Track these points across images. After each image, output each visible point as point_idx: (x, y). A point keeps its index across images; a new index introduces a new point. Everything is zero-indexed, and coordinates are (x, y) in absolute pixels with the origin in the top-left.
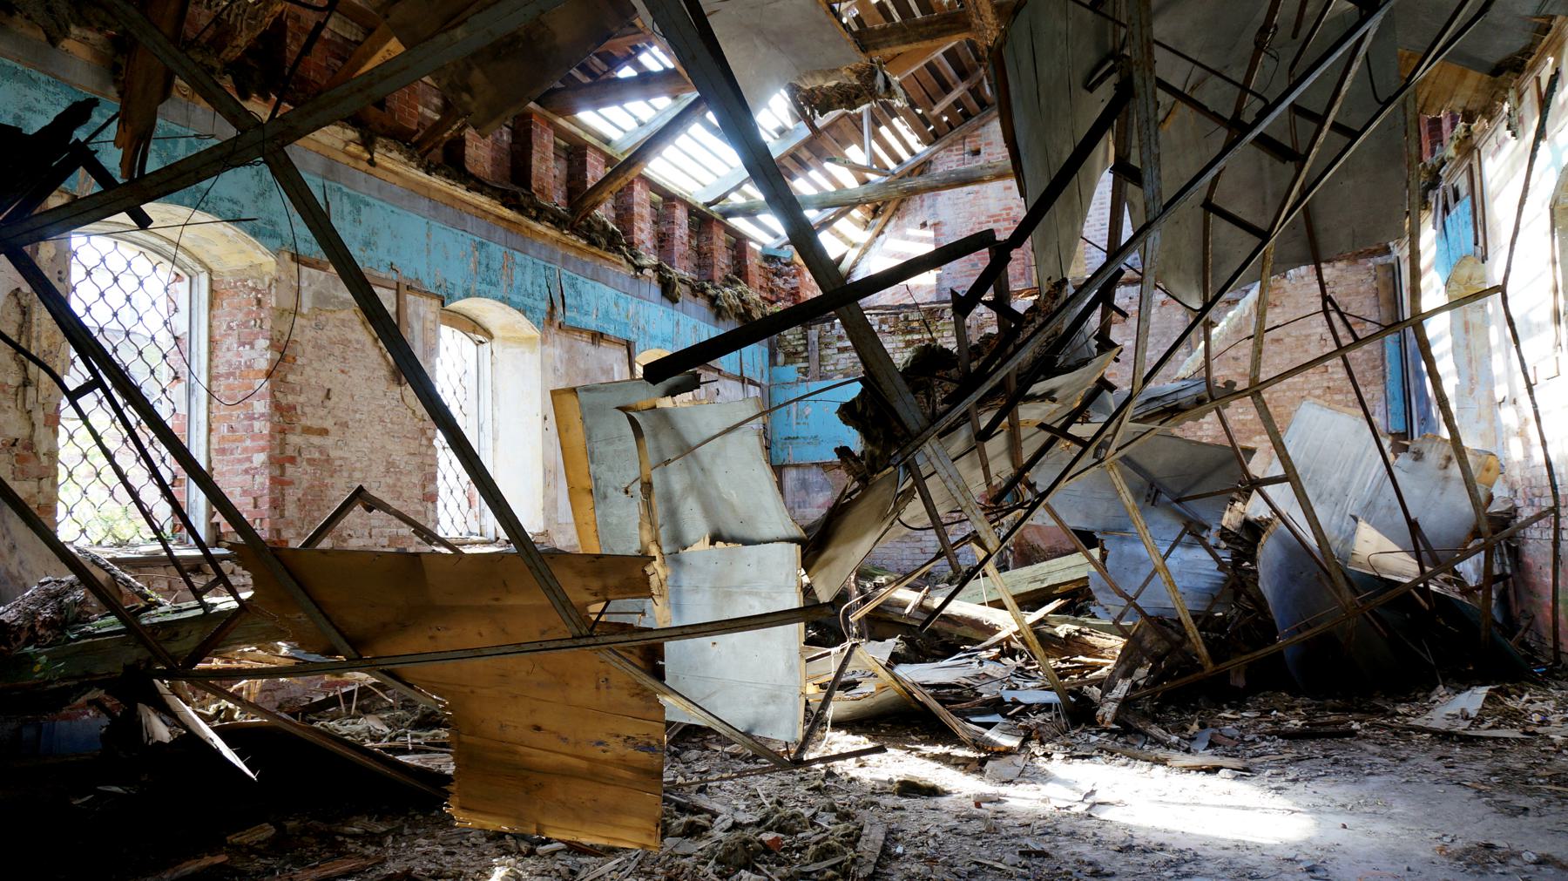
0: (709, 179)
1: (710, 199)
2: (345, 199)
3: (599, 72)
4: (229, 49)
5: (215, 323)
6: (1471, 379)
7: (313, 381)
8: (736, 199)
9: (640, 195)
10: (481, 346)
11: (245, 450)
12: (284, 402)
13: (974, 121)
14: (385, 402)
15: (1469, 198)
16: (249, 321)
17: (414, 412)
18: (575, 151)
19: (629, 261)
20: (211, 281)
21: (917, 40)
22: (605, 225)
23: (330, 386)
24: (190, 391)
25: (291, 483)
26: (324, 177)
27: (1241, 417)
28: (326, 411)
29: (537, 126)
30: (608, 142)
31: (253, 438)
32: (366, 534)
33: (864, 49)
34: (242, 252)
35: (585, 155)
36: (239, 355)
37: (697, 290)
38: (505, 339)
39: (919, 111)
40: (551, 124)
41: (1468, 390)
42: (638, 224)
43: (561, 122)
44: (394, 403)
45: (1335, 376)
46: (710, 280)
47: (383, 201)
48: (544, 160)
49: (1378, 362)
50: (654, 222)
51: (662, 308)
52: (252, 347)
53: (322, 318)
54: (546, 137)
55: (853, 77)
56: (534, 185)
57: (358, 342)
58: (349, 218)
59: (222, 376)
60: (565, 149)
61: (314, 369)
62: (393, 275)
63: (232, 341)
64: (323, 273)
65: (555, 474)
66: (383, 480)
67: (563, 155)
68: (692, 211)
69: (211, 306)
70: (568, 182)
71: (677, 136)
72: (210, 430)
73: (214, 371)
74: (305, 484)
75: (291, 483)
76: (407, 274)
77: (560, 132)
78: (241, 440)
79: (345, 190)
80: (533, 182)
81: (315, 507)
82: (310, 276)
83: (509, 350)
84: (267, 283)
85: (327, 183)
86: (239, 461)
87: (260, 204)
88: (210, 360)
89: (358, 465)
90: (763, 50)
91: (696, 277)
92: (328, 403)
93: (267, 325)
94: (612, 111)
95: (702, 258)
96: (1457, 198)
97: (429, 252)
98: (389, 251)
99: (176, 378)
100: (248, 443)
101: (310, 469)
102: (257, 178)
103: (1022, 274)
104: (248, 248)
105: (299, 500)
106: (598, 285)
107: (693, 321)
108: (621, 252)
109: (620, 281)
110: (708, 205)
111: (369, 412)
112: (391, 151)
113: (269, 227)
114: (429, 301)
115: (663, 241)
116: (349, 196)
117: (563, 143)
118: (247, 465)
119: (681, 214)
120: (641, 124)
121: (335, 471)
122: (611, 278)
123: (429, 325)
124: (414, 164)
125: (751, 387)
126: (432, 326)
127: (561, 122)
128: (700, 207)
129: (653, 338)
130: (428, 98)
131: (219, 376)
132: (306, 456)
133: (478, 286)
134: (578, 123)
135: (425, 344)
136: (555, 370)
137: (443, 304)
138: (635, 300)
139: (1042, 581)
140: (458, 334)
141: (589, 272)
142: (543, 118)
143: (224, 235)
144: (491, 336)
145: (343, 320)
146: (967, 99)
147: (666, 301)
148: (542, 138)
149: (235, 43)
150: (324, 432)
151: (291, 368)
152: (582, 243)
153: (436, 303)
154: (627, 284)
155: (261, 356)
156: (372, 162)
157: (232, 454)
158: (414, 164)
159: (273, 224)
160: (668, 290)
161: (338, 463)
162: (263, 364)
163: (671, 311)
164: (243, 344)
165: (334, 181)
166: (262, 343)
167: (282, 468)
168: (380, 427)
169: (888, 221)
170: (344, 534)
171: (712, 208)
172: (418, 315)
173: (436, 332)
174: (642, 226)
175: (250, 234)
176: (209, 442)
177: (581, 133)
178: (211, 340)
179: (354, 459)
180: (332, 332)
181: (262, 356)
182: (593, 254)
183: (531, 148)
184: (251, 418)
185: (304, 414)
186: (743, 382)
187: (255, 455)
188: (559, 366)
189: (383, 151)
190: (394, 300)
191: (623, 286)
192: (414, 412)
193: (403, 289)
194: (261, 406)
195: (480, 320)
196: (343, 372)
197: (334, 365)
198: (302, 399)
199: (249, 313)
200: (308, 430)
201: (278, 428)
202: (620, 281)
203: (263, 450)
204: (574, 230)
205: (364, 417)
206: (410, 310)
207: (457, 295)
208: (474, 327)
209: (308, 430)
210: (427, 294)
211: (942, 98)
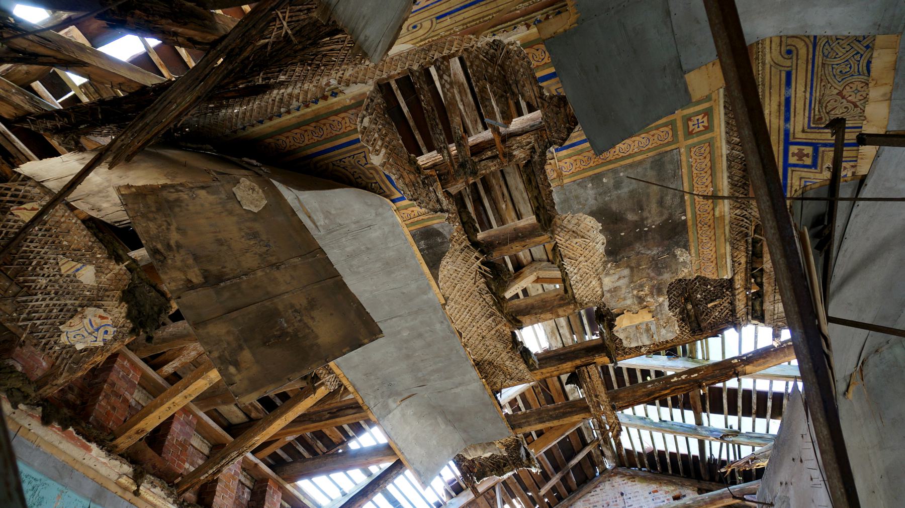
3: (320, 452)
13: (565, 502)
21: (549, 420)
29: (271, 488)
33: (513, 427)
39: (530, 494)
40: (281, 488)
43: (289, 487)
55: (503, 450)
71: (375, 494)
90: (443, 426)
112: (155, 487)
120: (344, 494)
124: (171, 500)
127: (289, 487)
130: (195, 459)
134: (298, 489)
142: (276, 482)
146: (560, 486)
149: (55, 383)
156: (136, 493)
158: (171, 500)
177: (301, 497)
183: (264, 504)
189: (149, 486)
211: (544, 484)
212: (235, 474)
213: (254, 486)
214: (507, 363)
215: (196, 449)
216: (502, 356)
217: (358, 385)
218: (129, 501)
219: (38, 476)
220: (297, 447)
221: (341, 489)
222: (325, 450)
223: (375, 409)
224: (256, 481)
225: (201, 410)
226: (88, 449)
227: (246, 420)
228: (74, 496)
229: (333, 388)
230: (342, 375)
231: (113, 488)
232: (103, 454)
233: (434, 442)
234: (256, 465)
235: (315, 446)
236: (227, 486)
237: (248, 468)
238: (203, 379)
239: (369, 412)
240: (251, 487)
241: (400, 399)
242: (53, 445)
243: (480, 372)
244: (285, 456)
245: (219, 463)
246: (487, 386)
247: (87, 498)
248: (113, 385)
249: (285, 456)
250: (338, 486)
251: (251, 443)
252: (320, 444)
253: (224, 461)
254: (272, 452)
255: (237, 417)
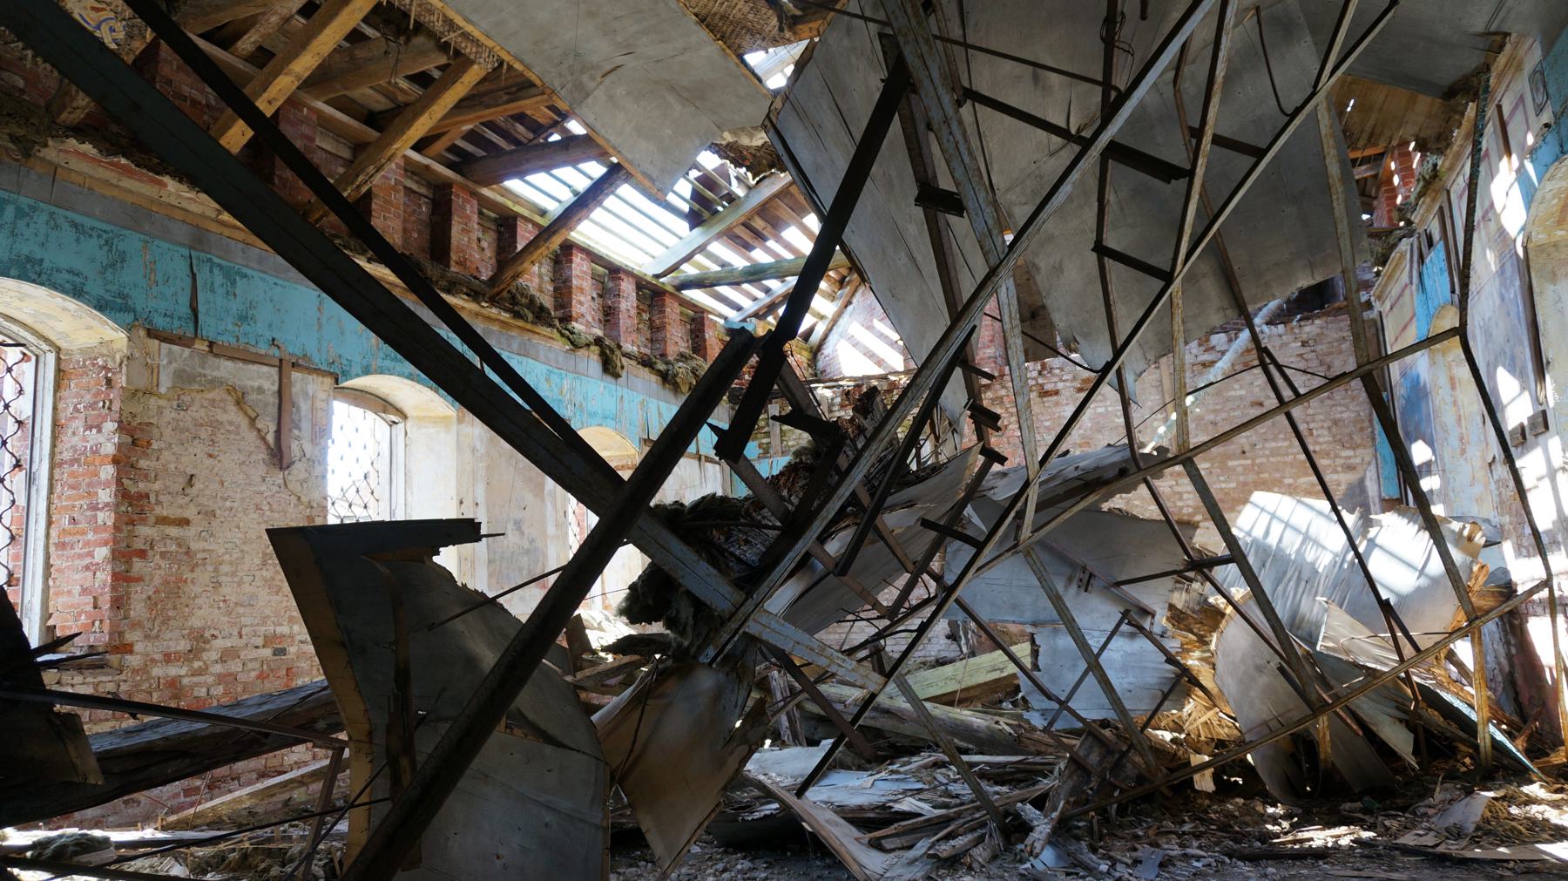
0: (658, 251)
1: (659, 271)
2: (216, 271)
4: (69, 110)
5: (61, 406)
6: (1461, 439)
7: (172, 466)
8: (689, 270)
9: (579, 268)
10: (395, 426)
11: (87, 544)
12: (133, 490)
14: (263, 488)
15: (1442, 243)
16: (96, 403)
17: (299, 498)
18: (505, 223)
19: (563, 335)
20: (58, 359)
22: (532, 299)
23: (194, 472)
24: (30, 480)
25: (139, 579)
26: (191, 248)
27: (1223, 485)
28: (187, 499)
29: (457, 196)
30: (543, 213)
31: (96, 531)
32: (235, 633)
34: (89, 328)
35: (515, 226)
36: (85, 439)
37: (646, 363)
38: (420, 419)
40: (474, 194)
41: (1458, 451)
42: (577, 297)
43: (485, 191)
44: (275, 489)
45: (1321, 440)
46: (663, 355)
47: (265, 272)
48: (466, 231)
49: (1366, 424)
50: (600, 296)
51: (602, 385)
52: (99, 431)
53: (187, 398)
54: (468, 207)
56: (454, 256)
57: (231, 423)
58: (220, 291)
59: (66, 463)
60: (495, 220)
61: (174, 454)
62: (276, 352)
63: (78, 424)
64: (187, 351)
65: (473, 563)
66: (258, 574)
67: (493, 227)
68: (641, 284)
69: (57, 387)
70: (498, 254)
72: (49, 523)
73: (58, 458)
74: (157, 581)
75: (139, 579)
76: (293, 348)
77: (484, 202)
78: (84, 533)
79: (217, 261)
80: (452, 254)
81: (170, 606)
82: (170, 351)
83: (423, 430)
84: (118, 361)
85: (194, 254)
86: (80, 556)
87: (109, 275)
88: (54, 446)
89: (227, 557)
91: (648, 351)
92: (188, 491)
93: (116, 407)
94: (539, 178)
95: (656, 331)
96: (1430, 244)
97: (320, 326)
98: (270, 326)
99: (18, 465)
100: (90, 536)
101: (162, 563)
102: (106, 248)
103: (992, 341)
104: (95, 323)
105: (149, 598)
106: (525, 359)
107: (641, 397)
108: (551, 326)
109: (552, 356)
110: (657, 276)
111: (243, 500)
113: (119, 301)
114: (320, 379)
115: (609, 315)
116: (221, 267)
117: (493, 215)
118: (87, 561)
119: (627, 287)
121: (197, 565)
122: (542, 353)
123: (319, 404)
125: (709, 465)
126: (323, 405)
127: (485, 191)
128: (649, 279)
129: (593, 415)
130: (333, 167)
131: (62, 463)
132: (159, 548)
133: (379, 362)
135: (313, 425)
136: (474, 450)
137: (337, 382)
138: (570, 375)
139: (1002, 670)
140: (370, 415)
141: (515, 346)
142: (464, 188)
143: (64, 309)
144: (405, 417)
145: (214, 400)
147: (609, 379)
148: (463, 208)
149: (75, 105)
150: (184, 522)
151: (144, 452)
152: (505, 316)
153: (329, 381)
154: (561, 359)
155: (108, 440)
157: (72, 548)
159: (124, 297)
160: (609, 367)
161: (200, 556)
162: (109, 449)
163: (613, 387)
164: (90, 428)
165: (203, 251)
166: (110, 426)
167: (129, 562)
168: (255, 516)
169: (855, 291)
170: (207, 635)
171: (661, 280)
172: (307, 394)
173: (328, 412)
174: (582, 299)
175: (95, 308)
176: (48, 535)
177: (510, 204)
178: (56, 425)
179: (222, 551)
180: (197, 413)
181: (109, 440)
182: (519, 327)
184: (94, 508)
185: (158, 503)
186: (700, 459)
187: (97, 549)
188: (478, 445)
190: (276, 378)
191: (557, 361)
192: (299, 498)
193: (286, 367)
194: (105, 496)
195: (391, 399)
196: (211, 456)
197: (199, 449)
198: (157, 486)
199: (98, 393)
200: (163, 521)
201: (125, 519)
202: (552, 356)
203: (106, 544)
204: (493, 301)
205: (236, 505)
206: (296, 389)
207: (354, 371)
208: (383, 406)
209: (163, 521)
210: (318, 371)
212: (396, 184)
213: (434, 194)
214: (751, 16)
215: (330, 153)
216: (739, 6)
217: (528, 60)
218: (243, 242)
219: (108, 227)
220: (486, 135)
221: (570, 187)
222: (531, 136)
223: (563, 93)
224: (436, 187)
225: (317, 98)
226: (165, 185)
227: (393, 105)
228: (165, 245)
229: (490, 66)
230: (498, 48)
231: (213, 227)
232: (184, 187)
233: (669, 132)
234: (427, 167)
235: (513, 132)
236: (387, 202)
237: (411, 169)
238: (286, 74)
239: (555, 98)
240: (431, 196)
241: (600, 73)
242: (112, 185)
243: (712, 31)
244: (470, 148)
245: (352, 183)
246: (728, 51)
247: (183, 245)
248: (169, 82)
249: (470, 148)
250: (565, 184)
251: (389, 153)
252: (520, 128)
253: (360, 179)
254: (449, 144)
255: (377, 101)
